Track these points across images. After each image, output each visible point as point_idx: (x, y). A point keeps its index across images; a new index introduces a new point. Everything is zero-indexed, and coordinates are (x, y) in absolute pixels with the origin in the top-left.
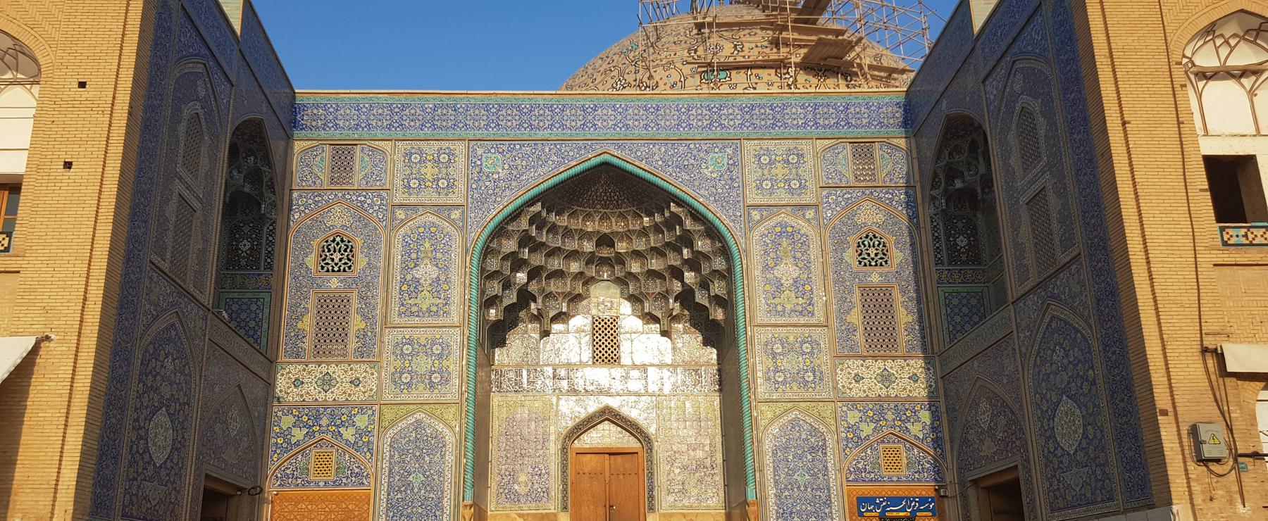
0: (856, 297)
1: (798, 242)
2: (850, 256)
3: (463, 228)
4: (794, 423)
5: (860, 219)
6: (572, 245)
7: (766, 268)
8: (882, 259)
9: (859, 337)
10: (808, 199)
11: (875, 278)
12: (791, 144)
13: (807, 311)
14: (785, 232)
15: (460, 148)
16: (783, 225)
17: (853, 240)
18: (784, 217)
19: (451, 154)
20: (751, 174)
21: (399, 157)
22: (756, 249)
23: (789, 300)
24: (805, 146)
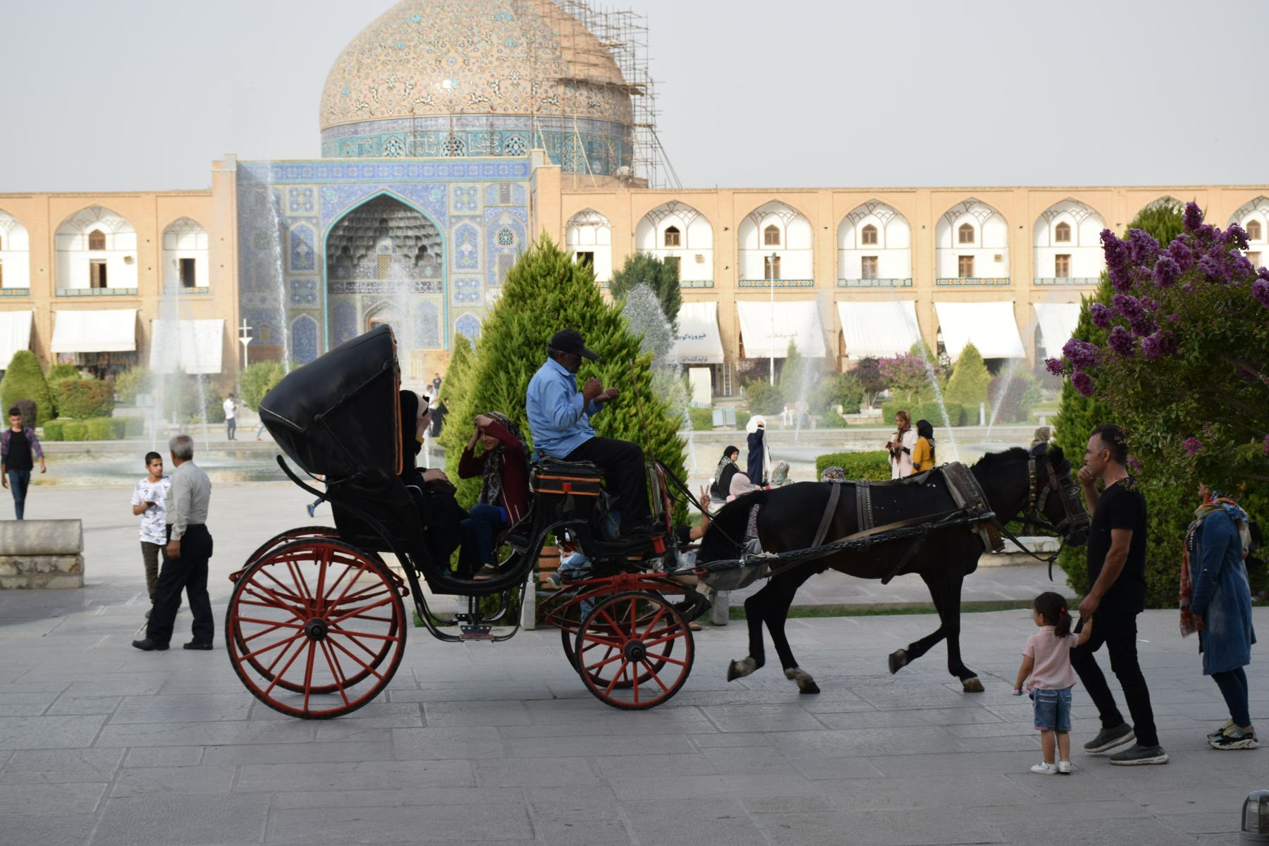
0: (497, 259)
1: (473, 234)
2: (496, 240)
3: (317, 225)
4: (467, 317)
5: (501, 223)
6: (368, 224)
7: (457, 246)
8: (510, 242)
9: (497, 278)
10: (478, 212)
11: (506, 250)
12: (471, 185)
13: (474, 266)
14: (466, 228)
15: (315, 188)
16: (466, 225)
17: (497, 232)
18: (467, 221)
19: (311, 191)
20: (452, 199)
21: (287, 192)
22: (453, 237)
23: (467, 261)
24: (478, 186)
